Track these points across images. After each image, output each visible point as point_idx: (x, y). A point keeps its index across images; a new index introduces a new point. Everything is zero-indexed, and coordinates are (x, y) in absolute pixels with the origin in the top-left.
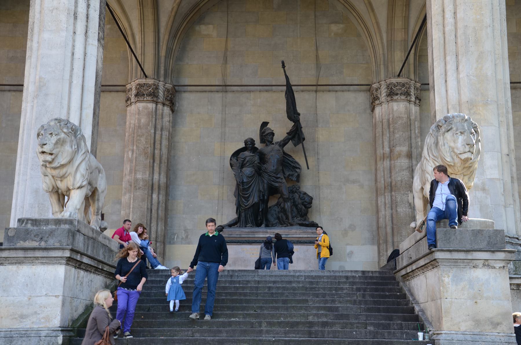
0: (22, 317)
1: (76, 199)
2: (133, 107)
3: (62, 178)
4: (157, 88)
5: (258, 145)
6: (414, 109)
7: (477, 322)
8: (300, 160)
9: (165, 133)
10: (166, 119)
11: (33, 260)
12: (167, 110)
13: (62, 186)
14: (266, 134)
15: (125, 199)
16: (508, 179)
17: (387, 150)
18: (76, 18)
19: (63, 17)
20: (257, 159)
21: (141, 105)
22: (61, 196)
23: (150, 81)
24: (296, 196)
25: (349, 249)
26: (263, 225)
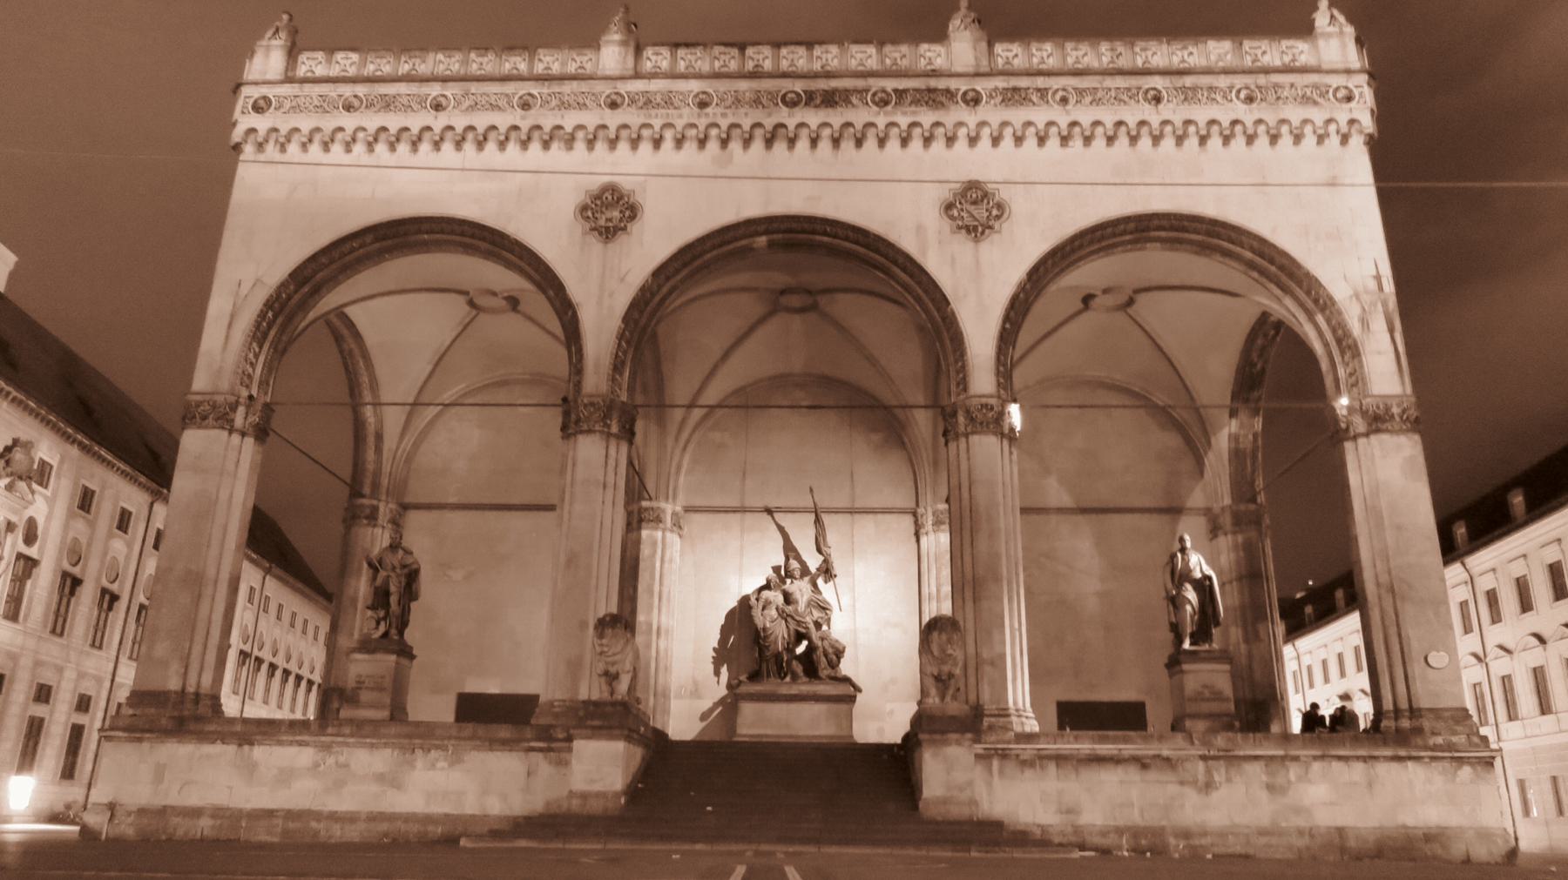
0: (592, 781)
3: (613, 664)
13: (613, 670)
17: (934, 590)
18: (605, 487)
20: (780, 599)
24: (826, 643)
25: (889, 707)
26: (788, 679)
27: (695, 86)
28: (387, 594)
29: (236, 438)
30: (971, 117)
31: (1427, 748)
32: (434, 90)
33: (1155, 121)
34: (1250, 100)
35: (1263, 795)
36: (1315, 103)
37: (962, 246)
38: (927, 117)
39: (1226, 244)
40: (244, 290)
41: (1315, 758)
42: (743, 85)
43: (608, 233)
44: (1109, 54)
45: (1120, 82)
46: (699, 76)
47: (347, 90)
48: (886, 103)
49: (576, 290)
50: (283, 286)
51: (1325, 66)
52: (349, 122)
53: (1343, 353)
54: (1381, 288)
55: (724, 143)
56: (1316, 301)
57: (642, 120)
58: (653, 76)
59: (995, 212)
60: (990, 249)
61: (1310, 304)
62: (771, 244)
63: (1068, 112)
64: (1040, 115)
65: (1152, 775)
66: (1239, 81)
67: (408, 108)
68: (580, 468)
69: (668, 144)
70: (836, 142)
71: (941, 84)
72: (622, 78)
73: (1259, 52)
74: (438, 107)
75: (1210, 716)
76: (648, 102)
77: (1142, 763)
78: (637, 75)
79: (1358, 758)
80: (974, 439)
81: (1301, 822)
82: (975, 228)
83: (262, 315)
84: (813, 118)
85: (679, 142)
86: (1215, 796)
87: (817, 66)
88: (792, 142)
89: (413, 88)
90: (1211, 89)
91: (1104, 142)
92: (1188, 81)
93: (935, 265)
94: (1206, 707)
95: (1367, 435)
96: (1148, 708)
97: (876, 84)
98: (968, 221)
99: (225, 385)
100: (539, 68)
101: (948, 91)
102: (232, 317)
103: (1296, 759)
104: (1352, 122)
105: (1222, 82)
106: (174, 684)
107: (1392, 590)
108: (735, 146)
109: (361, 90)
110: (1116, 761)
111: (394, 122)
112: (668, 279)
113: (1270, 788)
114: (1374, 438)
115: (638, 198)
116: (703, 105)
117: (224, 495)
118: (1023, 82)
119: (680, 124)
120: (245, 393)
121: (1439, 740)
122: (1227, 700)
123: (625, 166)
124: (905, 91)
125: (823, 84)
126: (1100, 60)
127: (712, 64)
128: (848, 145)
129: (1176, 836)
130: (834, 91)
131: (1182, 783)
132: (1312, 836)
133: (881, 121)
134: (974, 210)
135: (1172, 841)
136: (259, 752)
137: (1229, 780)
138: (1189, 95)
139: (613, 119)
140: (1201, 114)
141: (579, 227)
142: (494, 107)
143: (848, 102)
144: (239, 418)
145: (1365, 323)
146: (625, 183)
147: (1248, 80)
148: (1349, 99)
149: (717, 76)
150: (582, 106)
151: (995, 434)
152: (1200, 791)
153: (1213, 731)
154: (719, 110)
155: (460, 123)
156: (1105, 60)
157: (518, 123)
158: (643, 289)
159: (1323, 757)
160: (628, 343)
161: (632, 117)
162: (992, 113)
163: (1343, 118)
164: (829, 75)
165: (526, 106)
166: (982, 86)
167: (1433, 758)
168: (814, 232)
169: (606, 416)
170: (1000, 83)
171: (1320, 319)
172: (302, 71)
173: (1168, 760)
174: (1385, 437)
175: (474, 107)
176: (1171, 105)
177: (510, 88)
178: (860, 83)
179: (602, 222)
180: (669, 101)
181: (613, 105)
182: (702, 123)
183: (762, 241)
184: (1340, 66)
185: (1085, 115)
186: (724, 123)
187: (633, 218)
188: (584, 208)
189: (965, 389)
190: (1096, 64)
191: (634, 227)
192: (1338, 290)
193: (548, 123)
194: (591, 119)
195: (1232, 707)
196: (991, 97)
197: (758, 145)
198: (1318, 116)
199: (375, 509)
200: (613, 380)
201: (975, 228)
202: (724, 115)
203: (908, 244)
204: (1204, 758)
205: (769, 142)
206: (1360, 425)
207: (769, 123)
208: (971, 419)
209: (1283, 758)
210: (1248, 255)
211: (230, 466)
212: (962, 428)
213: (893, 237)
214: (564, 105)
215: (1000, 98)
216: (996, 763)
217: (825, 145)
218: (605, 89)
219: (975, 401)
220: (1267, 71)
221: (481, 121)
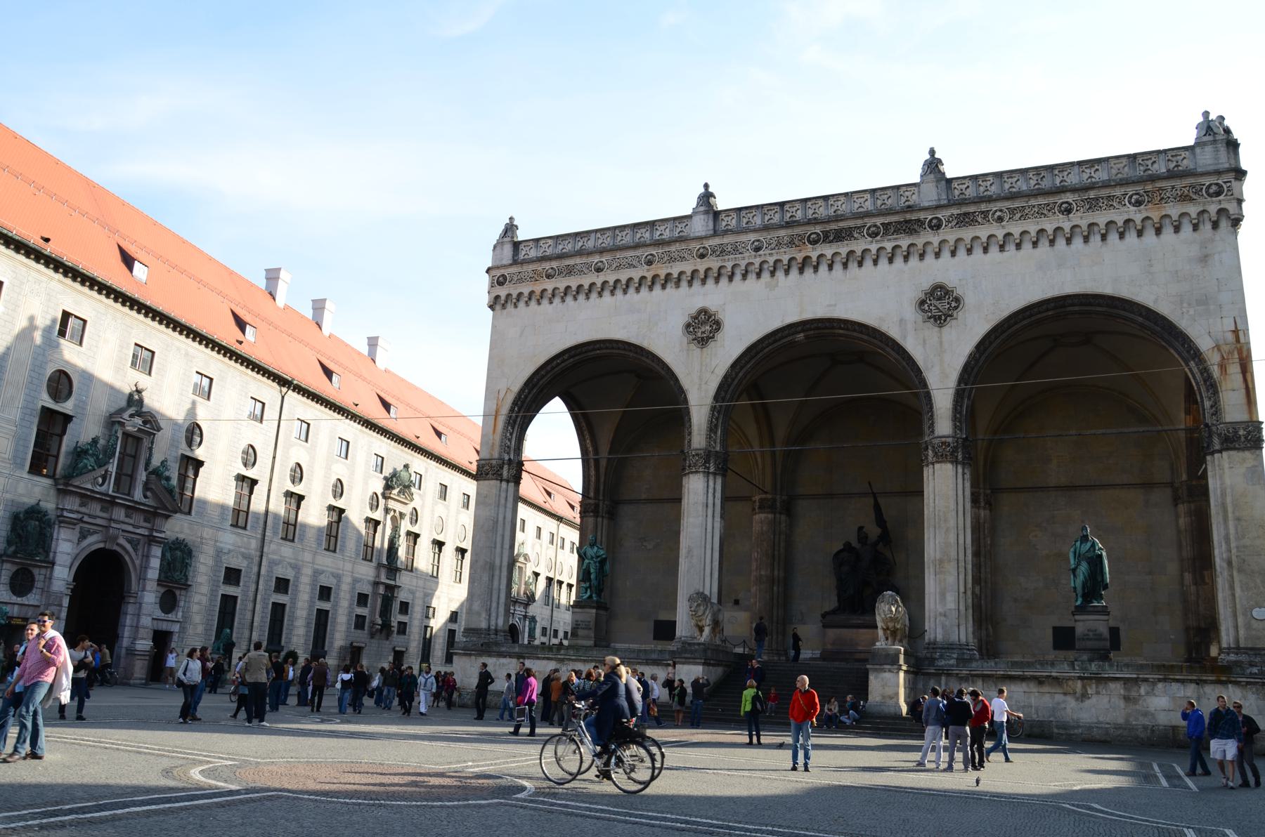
1: (707, 630)
2: (757, 517)
4: (774, 500)
5: (855, 544)
7: (884, 697)
9: (783, 537)
10: (783, 525)
11: (689, 663)
12: (783, 517)
14: (862, 535)
15: (753, 589)
16: (962, 608)
19: (700, 508)
21: (763, 516)
22: (701, 629)
23: (769, 496)
27: (752, 237)
28: (589, 573)
29: (504, 484)
30: (935, 239)
31: (1243, 675)
32: (596, 259)
33: (1067, 226)
34: (1138, 203)
35: (1122, 704)
36: (1191, 200)
37: (931, 331)
38: (904, 242)
39: (1122, 313)
41: (1160, 680)
42: (782, 233)
43: (703, 341)
44: (1035, 178)
46: (755, 231)
47: (547, 265)
48: (877, 234)
49: (685, 382)
50: (522, 391)
51: (1199, 170)
52: (549, 285)
53: (1208, 390)
54: (1238, 340)
55: (773, 273)
56: (1188, 352)
57: (720, 264)
58: (726, 232)
59: (953, 304)
60: (950, 332)
61: (1185, 354)
62: (807, 337)
63: (1003, 227)
64: (983, 232)
65: (1046, 689)
66: (1130, 190)
68: (692, 496)
69: (738, 277)
70: (845, 265)
71: (914, 217)
72: (706, 237)
73: (1149, 163)
74: (599, 270)
75: (1091, 650)
76: (721, 251)
77: (1040, 681)
78: (716, 233)
79: (1191, 681)
80: (937, 466)
81: (1146, 721)
82: (940, 317)
83: (512, 410)
84: (828, 250)
85: (744, 276)
86: (1087, 703)
87: (831, 212)
88: (816, 268)
89: (584, 260)
90: (1110, 198)
91: (1031, 246)
92: (1092, 194)
93: (912, 346)
94: (1089, 644)
95: (1220, 451)
96: (1051, 644)
97: (869, 222)
98: (935, 312)
99: (496, 455)
100: (656, 236)
101: (919, 220)
103: (1146, 680)
104: (1221, 211)
105: (1118, 192)
106: (484, 625)
107: (1230, 563)
108: (780, 274)
109: (555, 264)
110: (1022, 679)
111: (573, 282)
112: (742, 368)
113: (1127, 699)
114: (1225, 454)
115: (720, 316)
116: (757, 249)
117: (501, 518)
118: (971, 209)
119: (743, 264)
120: (507, 458)
121: (1255, 670)
122: (1105, 639)
124: (889, 224)
125: (834, 226)
126: (1028, 184)
127: (763, 219)
128: (853, 266)
129: (1058, 727)
130: (842, 230)
131: (1065, 694)
132: (1153, 731)
133: (874, 248)
134: (940, 304)
135: (1056, 730)
137: (1098, 693)
138: (1093, 205)
139: (702, 266)
140: (1101, 218)
142: (631, 266)
146: (713, 309)
147: (1139, 188)
148: (1218, 194)
149: (766, 228)
150: (683, 259)
151: (952, 462)
152: (1077, 699)
153: (1091, 660)
154: (768, 252)
155: (611, 279)
156: (1033, 182)
157: (645, 274)
158: (726, 377)
159: (1165, 680)
160: (719, 412)
161: (713, 263)
162: (950, 234)
163: (1213, 209)
164: (838, 218)
165: (649, 263)
166: (942, 215)
167: (1248, 683)
168: (833, 328)
169: (707, 461)
170: (956, 211)
171: (1192, 364)
172: (521, 257)
173: (1056, 678)
174: (1232, 453)
175: (618, 268)
176: (1079, 214)
177: (638, 252)
178: (859, 222)
179: (699, 335)
180: (736, 250)
181: (702, 256)
182: (757, 261)
184: (1211, 168)
185: (1016, 229)
186: (771, 260)
187: (718, 329)
188: (688, 326)
189: (933, 432)
190: (1024, 188)
191: (719, 336)
192: (1204, 344)
193: (662, 273)
194: (688, 267)
195: (1108, 644)
196: (949, 222)
197: (794, 272)
198: (1193, 210)
199: (597, 506)
200: (709, 437)
201: (940, 317)
202: (771, 254)
203: (894, 333)
204: (1080, 678)
205: (801, 270)
206: (1216, 443)
207: (799, 257)
208: (936, 454)
209: (1136, 681)
210: (1140, 319)
211: (503, 501)
212: (930, 459)
213: (884, 329)
214: (672, 260)
215: (954, 223)
216: (943, 678)
217: (838, 267)
218: (695, 246)
219: (937, 441)
220: (1153, 178)
221: (624, 276)
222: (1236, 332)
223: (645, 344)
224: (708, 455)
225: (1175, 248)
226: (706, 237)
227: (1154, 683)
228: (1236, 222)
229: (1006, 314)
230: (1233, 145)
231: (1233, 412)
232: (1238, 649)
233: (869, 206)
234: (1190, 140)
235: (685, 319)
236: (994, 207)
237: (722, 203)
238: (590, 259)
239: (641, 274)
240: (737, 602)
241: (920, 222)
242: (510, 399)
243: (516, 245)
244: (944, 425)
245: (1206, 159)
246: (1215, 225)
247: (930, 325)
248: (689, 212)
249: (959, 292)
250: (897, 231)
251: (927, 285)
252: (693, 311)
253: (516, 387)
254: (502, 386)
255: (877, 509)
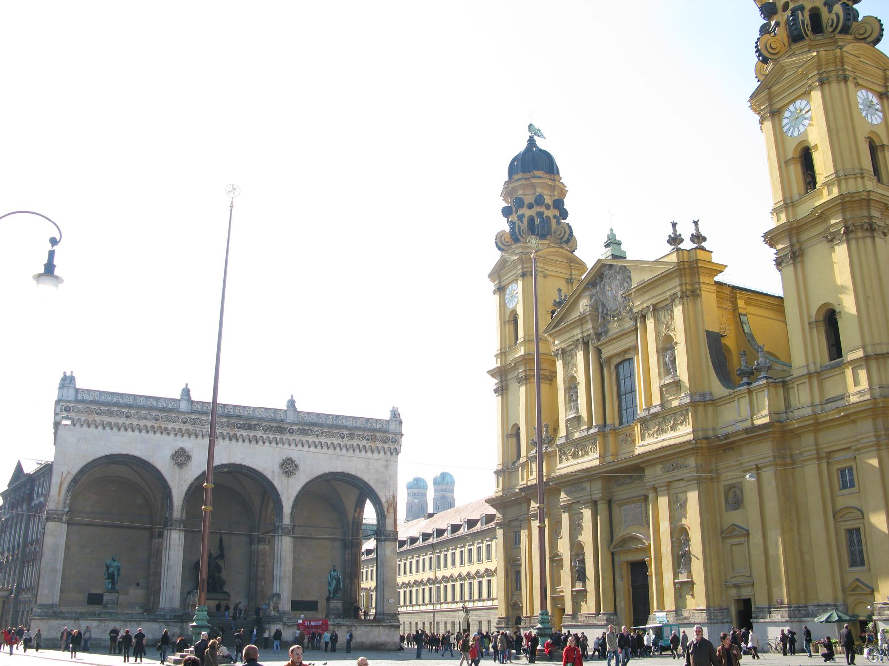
6: (267, 547)
8: (223, 566)
28: (113, 575)
34: (368, 440)
37: (284, 478)
38: (278, 437)
40: (64, 475)
42: (224, 420)
43: (181, 465)
45: (334, 430)
47: (97, 407)
49: (171, 484)
50: (77, 474)
52: (98, 419)
58: (198, 413)
64: (310, 439)
66: (366, 433)
67: (117, 416)
68: (173, 542)
70: (250, 441)
74: (128, 417)
87: (246, 414)
88: (237, 440)
90: (359, 435)
93: (276, 483)
97: (264, 424)
100: (160, 405)
102: (61, 484)
105: (362, 433)
109: (102, 408)
111: (113, 420)
123: (187, 443)
134: (289, 467)
136: (80, 622)
138: (352, 436)
140: (355, 443)
141: (172, 463)
142: (146, 419)
143: (255, 429)
144: (64, 518)
145: (388, 509)
146: (187, 450)
150: (174, 422)
153: (336, 618)
162: (298, 438)
165: (156, 420)
166: (295, 428)
175: (139, 418)
180: (201, 423)
181: (184, 423)
183: (226, 469)
188: (173, 456)
192: (383, 500)
193: (163, 426)
197: (227, 439)
198: (386, 446)
203: (269, 476)
205: (230, 439)
207: (231, 433)
208: (282, 530)
214: (168, 421)
220: (375, 430)
221: (142, 423)
222: (393, 497)
223: (151, 461)
224: (181, 522)
225: (378, 459)
226: (187, 413)
227: (356, 626)
228: (397, 454)
229: (314, 476)
230: (401, 422)
231: (390, 528)
232: (383, 614)
233: (264, 415)
234: (388, 418)
235: (173, 452)
236: (316, 429)
237: (194, 397)
238: (123, 410)
239: (151, 424)
240: (138, 584)
241: (286, 429)
242: (70, 478)
243: (77, 390)
244: (287, 521)
245: (392, 427)
246: (391, 454)
247: (284, 475)
248: (179, 397)
249: (297, 463)
250: (275, 431)
251: (285, 457)
252: (176, 449)
253: (74, 472)
254: (65, 469)
255: (221, 540)
